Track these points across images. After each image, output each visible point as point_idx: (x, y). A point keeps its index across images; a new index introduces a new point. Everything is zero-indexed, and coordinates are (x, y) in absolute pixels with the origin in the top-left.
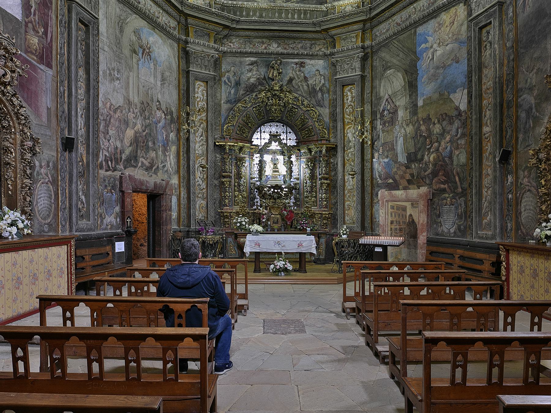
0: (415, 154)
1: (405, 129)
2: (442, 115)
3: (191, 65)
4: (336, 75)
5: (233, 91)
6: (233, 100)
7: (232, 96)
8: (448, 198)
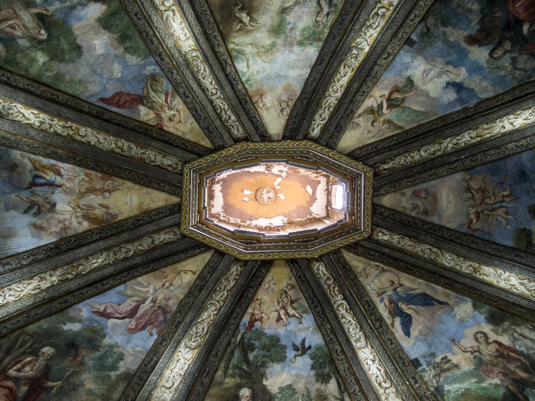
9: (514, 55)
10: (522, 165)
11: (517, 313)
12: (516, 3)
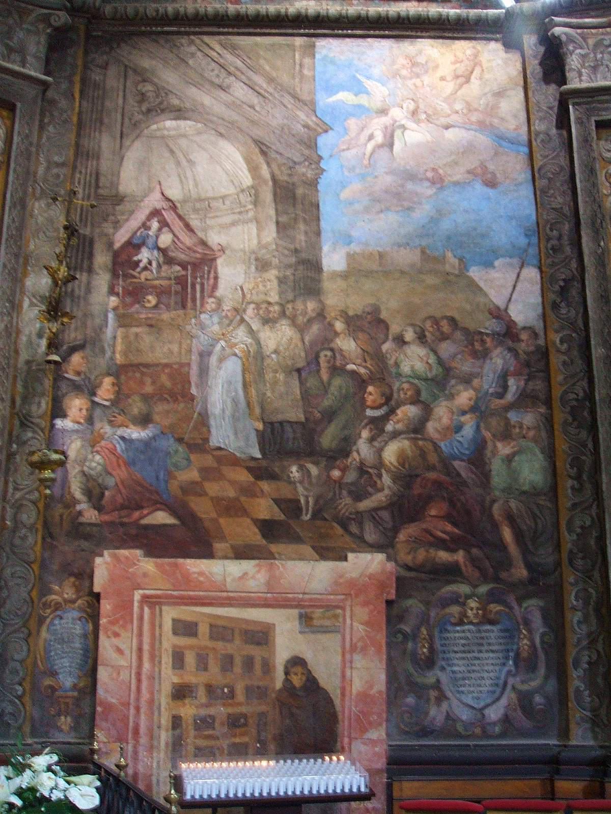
0: (309, 430)
1: (251, 332)
2: (436, 322)
8: (468, 597)
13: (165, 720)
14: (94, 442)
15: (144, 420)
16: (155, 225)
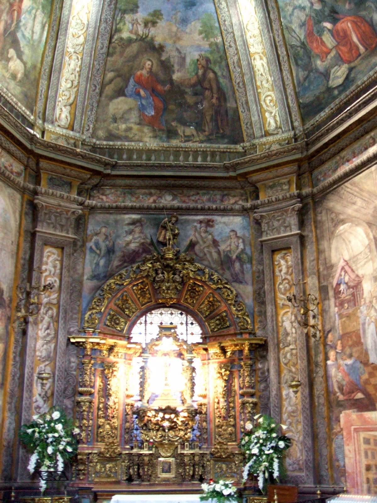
3: (39, 224)
4: (261, 236)
5: (102, 262)
6: (102, 275)
7: (101, 270)
9: (307, 10)
10: (202, 4)
11: (54, 8)
12: (351, 24)
13: (365, 480)
14: (338, 367)
15: (350, 356)
16: (343, 273)
